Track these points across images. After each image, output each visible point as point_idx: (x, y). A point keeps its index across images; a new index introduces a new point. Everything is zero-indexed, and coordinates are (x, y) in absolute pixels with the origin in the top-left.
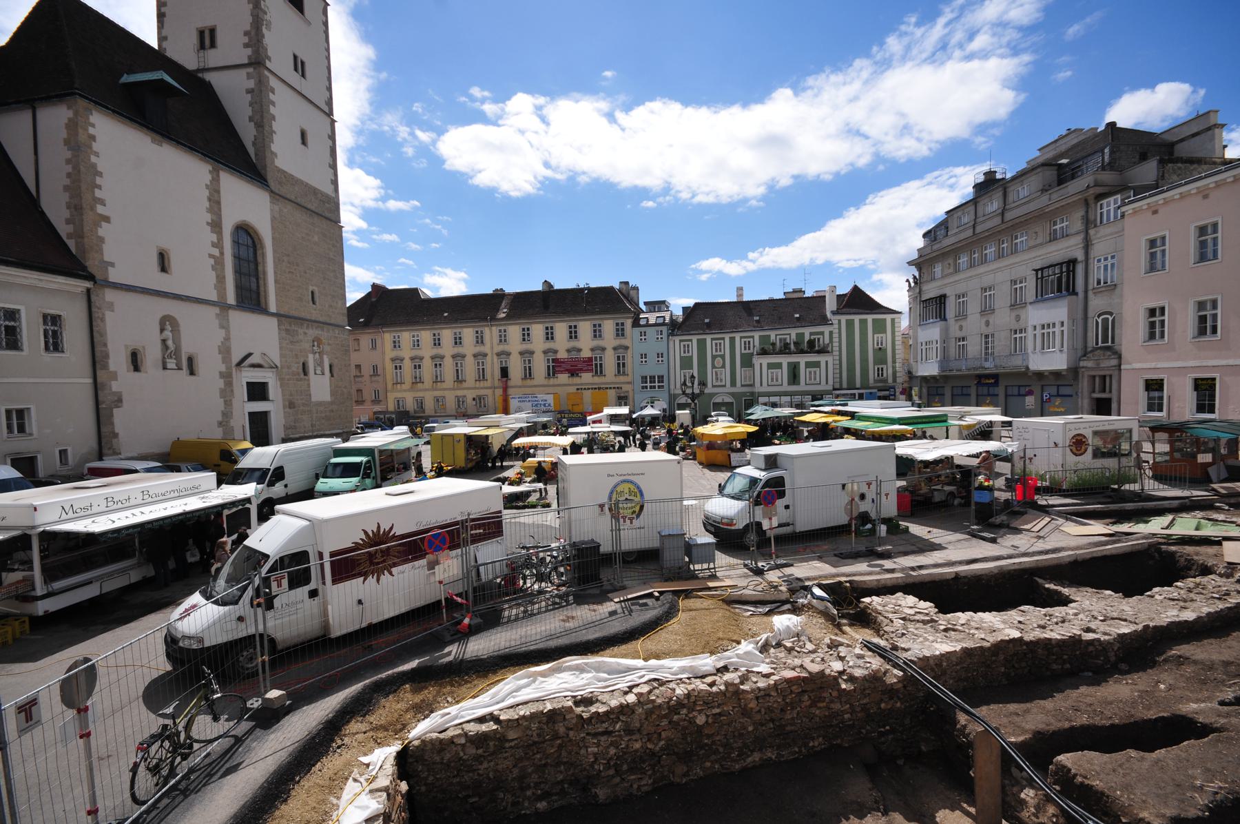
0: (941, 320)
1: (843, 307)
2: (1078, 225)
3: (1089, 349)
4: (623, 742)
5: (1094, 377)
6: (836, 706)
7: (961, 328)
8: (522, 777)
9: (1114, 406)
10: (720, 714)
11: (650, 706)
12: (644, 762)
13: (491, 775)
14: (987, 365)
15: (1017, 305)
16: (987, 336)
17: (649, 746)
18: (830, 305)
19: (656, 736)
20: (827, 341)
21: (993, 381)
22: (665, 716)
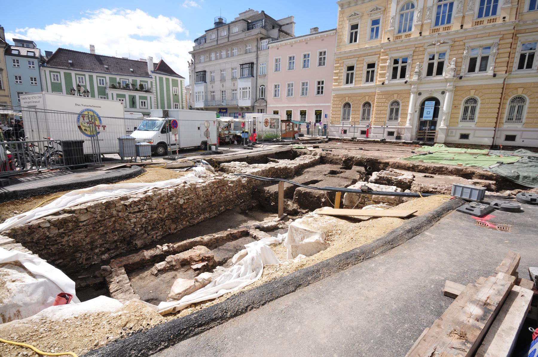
1: (157, 70)
2: (255, 49)
4: (148, 215)
6: (228, 193)
7: (212, 87)
8: (92, 243)
10: (188, 198)
11: (159, 197)
12: (158, 224)
13: (71, 244)
14: (223, 104)
15: (234, 79)
16: (223, 92)
17: (161, 216)
18: (150, 68)
19: (163, 211)
20: (150, 86)
22: (167, 201)
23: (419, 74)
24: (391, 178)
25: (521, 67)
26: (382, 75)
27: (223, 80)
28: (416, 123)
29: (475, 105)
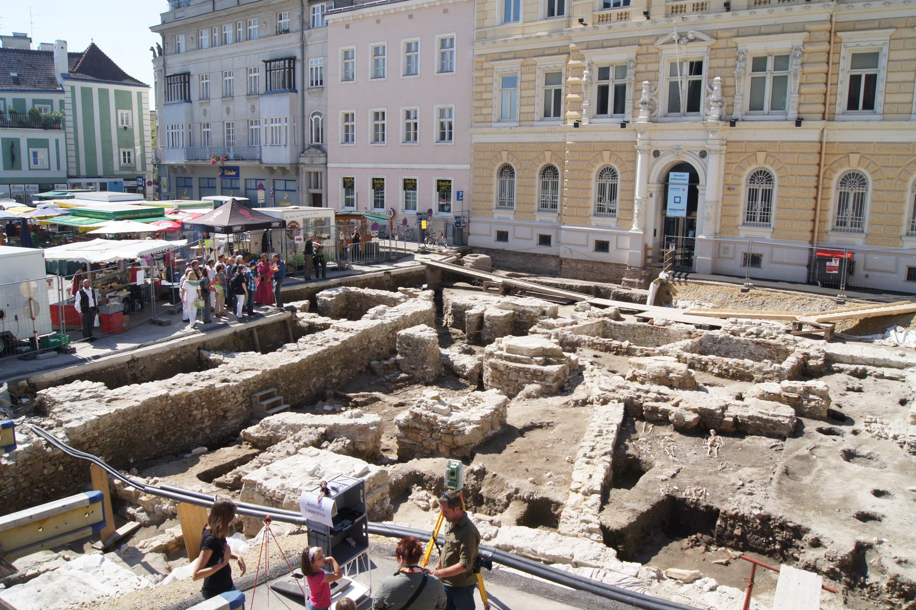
0: (186, 101)
1: (78, 71)
2: (296, 25)
3: (306, 147)
5: (310, 173)
9: (324, 200)
15: (252, 94)
16: (228, 125)
18: (61, 66)
21: (234, 173)
23: (651, 106)
24: (435, 418)
25: (852, 104)
26: (577, 106)
27: (228, 96)
28: (654, 222)
29: (768, 187)
